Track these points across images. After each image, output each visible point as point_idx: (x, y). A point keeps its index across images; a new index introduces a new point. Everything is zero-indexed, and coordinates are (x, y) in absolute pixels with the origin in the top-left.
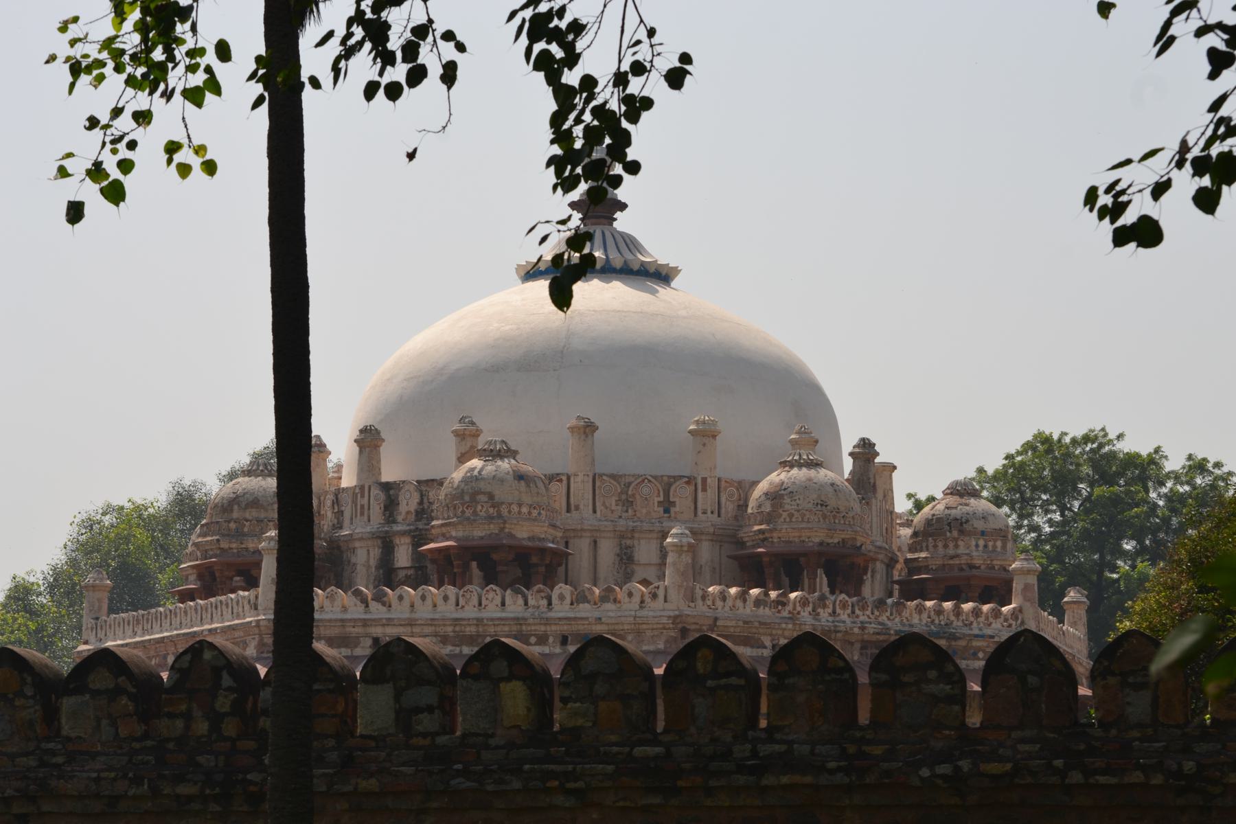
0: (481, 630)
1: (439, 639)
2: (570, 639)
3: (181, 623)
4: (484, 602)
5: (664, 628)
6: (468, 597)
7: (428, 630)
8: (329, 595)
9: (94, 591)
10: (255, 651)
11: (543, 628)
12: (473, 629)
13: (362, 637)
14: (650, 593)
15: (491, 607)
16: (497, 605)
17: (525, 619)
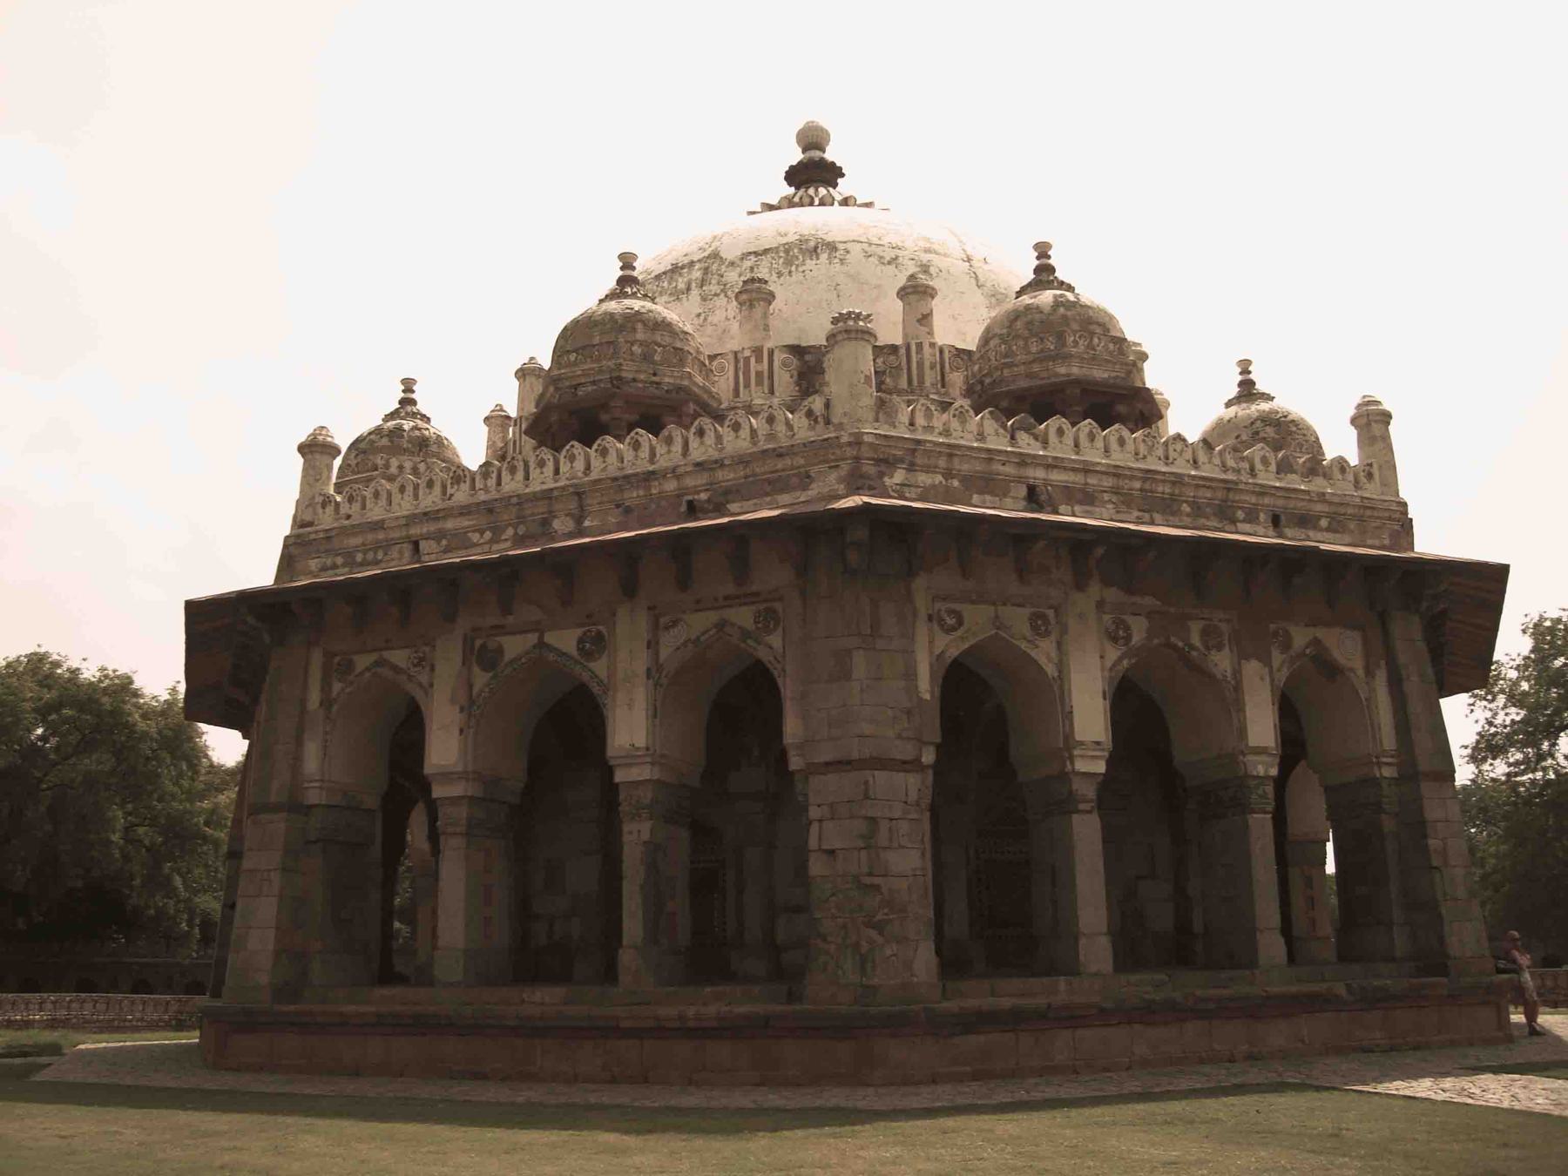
0: (1177, 492)
1: (1122, 499)
2: (1283, 518)
3: (588, 468)
4: (1172, 455)
5: (1390, 519)
6: (1150, 443)
7: (1108, 482)
9: (322, 453)
10: (842, 486)
11: (1254, 500)
13: (1013, 482)
14: (1364, 471)
15: (1180, 462)
16: (1188, 461)
17: (1237, 484)
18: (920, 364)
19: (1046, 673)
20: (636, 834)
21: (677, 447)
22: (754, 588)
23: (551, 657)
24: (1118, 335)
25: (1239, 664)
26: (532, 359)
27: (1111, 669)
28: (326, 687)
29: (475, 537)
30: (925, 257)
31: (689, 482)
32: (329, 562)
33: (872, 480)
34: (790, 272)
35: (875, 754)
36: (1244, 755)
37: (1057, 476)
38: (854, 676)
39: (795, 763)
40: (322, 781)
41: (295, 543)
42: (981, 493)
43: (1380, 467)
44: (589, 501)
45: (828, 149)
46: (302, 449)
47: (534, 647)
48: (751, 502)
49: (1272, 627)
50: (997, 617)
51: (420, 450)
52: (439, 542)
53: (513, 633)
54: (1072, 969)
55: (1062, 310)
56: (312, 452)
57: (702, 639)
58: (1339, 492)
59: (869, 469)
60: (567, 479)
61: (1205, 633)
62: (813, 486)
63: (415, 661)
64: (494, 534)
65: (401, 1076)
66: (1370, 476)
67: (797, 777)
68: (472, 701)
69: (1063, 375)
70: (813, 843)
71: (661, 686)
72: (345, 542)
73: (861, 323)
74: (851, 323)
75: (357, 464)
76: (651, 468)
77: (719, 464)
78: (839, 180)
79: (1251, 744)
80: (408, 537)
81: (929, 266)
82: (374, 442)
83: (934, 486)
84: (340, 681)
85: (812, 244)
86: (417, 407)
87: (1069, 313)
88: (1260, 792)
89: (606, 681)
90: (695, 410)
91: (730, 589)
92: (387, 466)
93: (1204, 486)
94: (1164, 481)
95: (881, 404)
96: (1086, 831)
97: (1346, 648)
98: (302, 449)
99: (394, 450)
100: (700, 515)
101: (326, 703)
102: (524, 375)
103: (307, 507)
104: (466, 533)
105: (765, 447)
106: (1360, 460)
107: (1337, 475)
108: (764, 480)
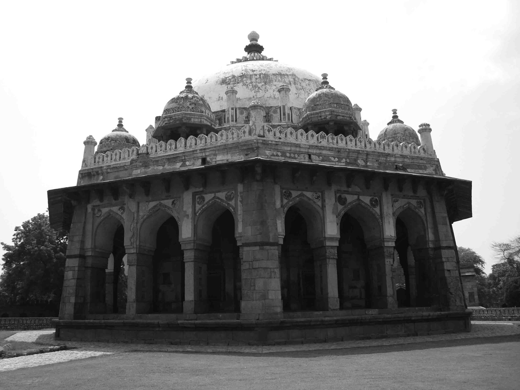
10: (434, 172)
28: (282, 201)
29: (333, 159)
31: (398, 160)
41: (262, 143)
44: (369, 157)
57: (405, 206)
62: (427, 170)
63: (316, 197)
65: (342, 341)
74: (427, 127)
80: (308, 152)
84: (286, 199)
100: (399, 170)
102: (233, 92)
108: (416, 165)
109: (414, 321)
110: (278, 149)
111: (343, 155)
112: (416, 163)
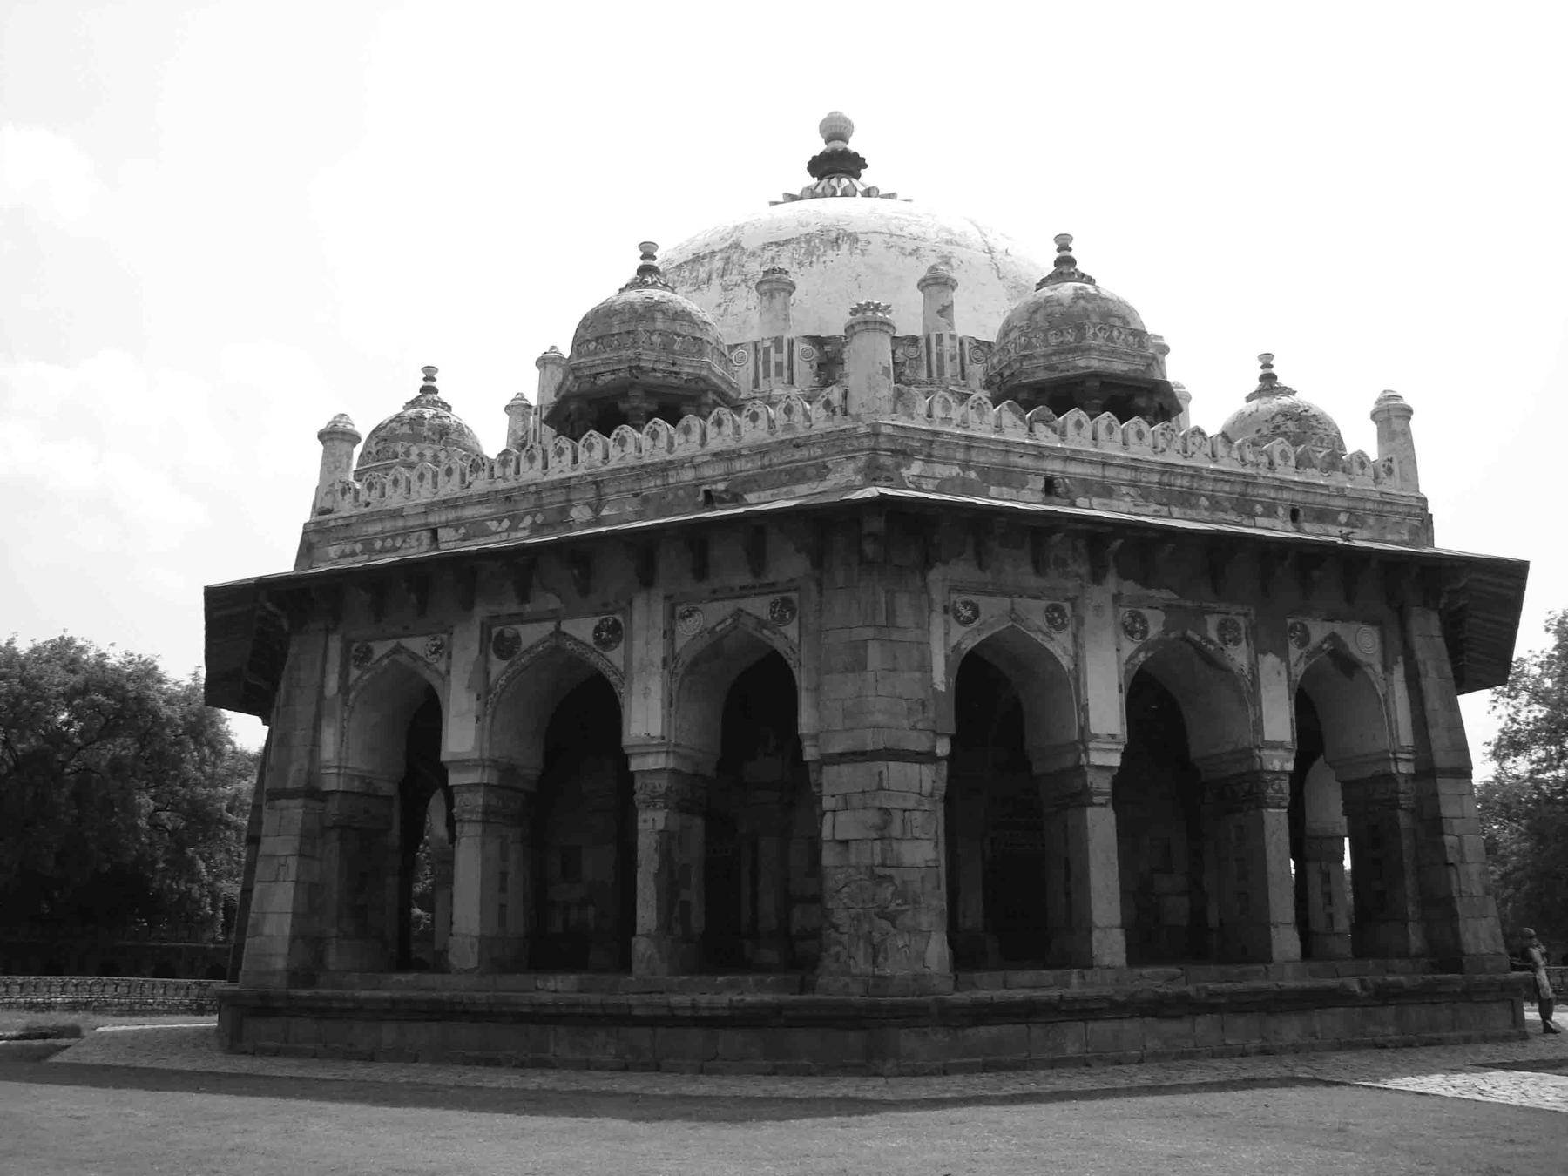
0: (1195, 485)
2: (1302, 513)
3: (606, 457)
4: (1191, 448)
5: (1409, 514)
6: (1169, 437)
7: (1126, 475)
8: (975, 404)
9: (343, 440)
10: (859, 477)
11: (1272, 494)
12: (1186, 482)
13: (1030, 474)
14: (1384, 466)
15: (1199, 455)
16: (1207, 455)
17: (1255, 477)
18: (940, 356)
19: (1063, 668)
20: (651, 823)
21: (695, 437)
22: (771, 579)
23: (569, 645)
24: (1138, 328)
25: (1256, 657)
26: (553, 347)
27: (1127, 663)
28: (344, 674)
29: (495, 523)
30: (947, 249)
31: (707, 472)
32: (348, 549)
33: (888, 471)
34: (811, 263)
35: (888, 747)
36: (1260, 749)
37: (1076, 469)
38: (869, 668)
39: (810, 753)
40: (339, 767)
42: (999, 485)
43: (1400, 462)
44: (607, 490)
45: (851, 140)
46: (323, 436)
47: (551, 635)
48: (769, 492)
49: (1290, 621)
50: (1013, 609)
51: (441, 438)
52: (457, 531)
53: (531, 621)
54: (1085, 962)
55: (1082, 302)
56: (332, 439)
57: (718, 629)
58: (1359, 487)
59: (886, 460)
60: (585, 468)
61: (1222, 627)
62: (830, 476)
63: (433, 649)
64: (511, 521)
65: (416, 1061)
66: (1390, 471)
67: (811, 767)
68: (488, 692)
69: (1083, 368)
70: (826, 833)
71: (677, 674)
72: (364, 529)
73: (880, 314)
74: (870, 314)
75: (378, 452)
76: (670, 457)
77: (737, 454)
78: (862, 171)
79: (1266, 739)
80: (426, 525)
81: (950, 258)
82: (395, 430)
83: (950, 479)
84: (358, 667)
85: (834, 235)
86: (439, 395)
87: (1089, 306)
88: (1276, 787)
89: (622, 669)
90: (714, 401)
91: (746, 579)
92: (408, 453)
93: (1222, 480)
94: (1183, 475)
95: (899, 395)
96: (1101, 825)
97: (1364, 643)
98: (323, 436)
99: (416, 438)
100: (717, 505)
101: (344, 689)
103: (327, 494)
104: (484, 521)
105: (782, 438)
106: (1379, 455)
107: (1356, 469)
108: (781, 471)
109: (651, 1022)
110: (352, 537)
111: (524, 505)
112: (780, 464)
